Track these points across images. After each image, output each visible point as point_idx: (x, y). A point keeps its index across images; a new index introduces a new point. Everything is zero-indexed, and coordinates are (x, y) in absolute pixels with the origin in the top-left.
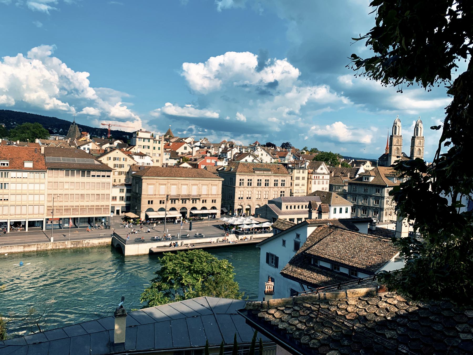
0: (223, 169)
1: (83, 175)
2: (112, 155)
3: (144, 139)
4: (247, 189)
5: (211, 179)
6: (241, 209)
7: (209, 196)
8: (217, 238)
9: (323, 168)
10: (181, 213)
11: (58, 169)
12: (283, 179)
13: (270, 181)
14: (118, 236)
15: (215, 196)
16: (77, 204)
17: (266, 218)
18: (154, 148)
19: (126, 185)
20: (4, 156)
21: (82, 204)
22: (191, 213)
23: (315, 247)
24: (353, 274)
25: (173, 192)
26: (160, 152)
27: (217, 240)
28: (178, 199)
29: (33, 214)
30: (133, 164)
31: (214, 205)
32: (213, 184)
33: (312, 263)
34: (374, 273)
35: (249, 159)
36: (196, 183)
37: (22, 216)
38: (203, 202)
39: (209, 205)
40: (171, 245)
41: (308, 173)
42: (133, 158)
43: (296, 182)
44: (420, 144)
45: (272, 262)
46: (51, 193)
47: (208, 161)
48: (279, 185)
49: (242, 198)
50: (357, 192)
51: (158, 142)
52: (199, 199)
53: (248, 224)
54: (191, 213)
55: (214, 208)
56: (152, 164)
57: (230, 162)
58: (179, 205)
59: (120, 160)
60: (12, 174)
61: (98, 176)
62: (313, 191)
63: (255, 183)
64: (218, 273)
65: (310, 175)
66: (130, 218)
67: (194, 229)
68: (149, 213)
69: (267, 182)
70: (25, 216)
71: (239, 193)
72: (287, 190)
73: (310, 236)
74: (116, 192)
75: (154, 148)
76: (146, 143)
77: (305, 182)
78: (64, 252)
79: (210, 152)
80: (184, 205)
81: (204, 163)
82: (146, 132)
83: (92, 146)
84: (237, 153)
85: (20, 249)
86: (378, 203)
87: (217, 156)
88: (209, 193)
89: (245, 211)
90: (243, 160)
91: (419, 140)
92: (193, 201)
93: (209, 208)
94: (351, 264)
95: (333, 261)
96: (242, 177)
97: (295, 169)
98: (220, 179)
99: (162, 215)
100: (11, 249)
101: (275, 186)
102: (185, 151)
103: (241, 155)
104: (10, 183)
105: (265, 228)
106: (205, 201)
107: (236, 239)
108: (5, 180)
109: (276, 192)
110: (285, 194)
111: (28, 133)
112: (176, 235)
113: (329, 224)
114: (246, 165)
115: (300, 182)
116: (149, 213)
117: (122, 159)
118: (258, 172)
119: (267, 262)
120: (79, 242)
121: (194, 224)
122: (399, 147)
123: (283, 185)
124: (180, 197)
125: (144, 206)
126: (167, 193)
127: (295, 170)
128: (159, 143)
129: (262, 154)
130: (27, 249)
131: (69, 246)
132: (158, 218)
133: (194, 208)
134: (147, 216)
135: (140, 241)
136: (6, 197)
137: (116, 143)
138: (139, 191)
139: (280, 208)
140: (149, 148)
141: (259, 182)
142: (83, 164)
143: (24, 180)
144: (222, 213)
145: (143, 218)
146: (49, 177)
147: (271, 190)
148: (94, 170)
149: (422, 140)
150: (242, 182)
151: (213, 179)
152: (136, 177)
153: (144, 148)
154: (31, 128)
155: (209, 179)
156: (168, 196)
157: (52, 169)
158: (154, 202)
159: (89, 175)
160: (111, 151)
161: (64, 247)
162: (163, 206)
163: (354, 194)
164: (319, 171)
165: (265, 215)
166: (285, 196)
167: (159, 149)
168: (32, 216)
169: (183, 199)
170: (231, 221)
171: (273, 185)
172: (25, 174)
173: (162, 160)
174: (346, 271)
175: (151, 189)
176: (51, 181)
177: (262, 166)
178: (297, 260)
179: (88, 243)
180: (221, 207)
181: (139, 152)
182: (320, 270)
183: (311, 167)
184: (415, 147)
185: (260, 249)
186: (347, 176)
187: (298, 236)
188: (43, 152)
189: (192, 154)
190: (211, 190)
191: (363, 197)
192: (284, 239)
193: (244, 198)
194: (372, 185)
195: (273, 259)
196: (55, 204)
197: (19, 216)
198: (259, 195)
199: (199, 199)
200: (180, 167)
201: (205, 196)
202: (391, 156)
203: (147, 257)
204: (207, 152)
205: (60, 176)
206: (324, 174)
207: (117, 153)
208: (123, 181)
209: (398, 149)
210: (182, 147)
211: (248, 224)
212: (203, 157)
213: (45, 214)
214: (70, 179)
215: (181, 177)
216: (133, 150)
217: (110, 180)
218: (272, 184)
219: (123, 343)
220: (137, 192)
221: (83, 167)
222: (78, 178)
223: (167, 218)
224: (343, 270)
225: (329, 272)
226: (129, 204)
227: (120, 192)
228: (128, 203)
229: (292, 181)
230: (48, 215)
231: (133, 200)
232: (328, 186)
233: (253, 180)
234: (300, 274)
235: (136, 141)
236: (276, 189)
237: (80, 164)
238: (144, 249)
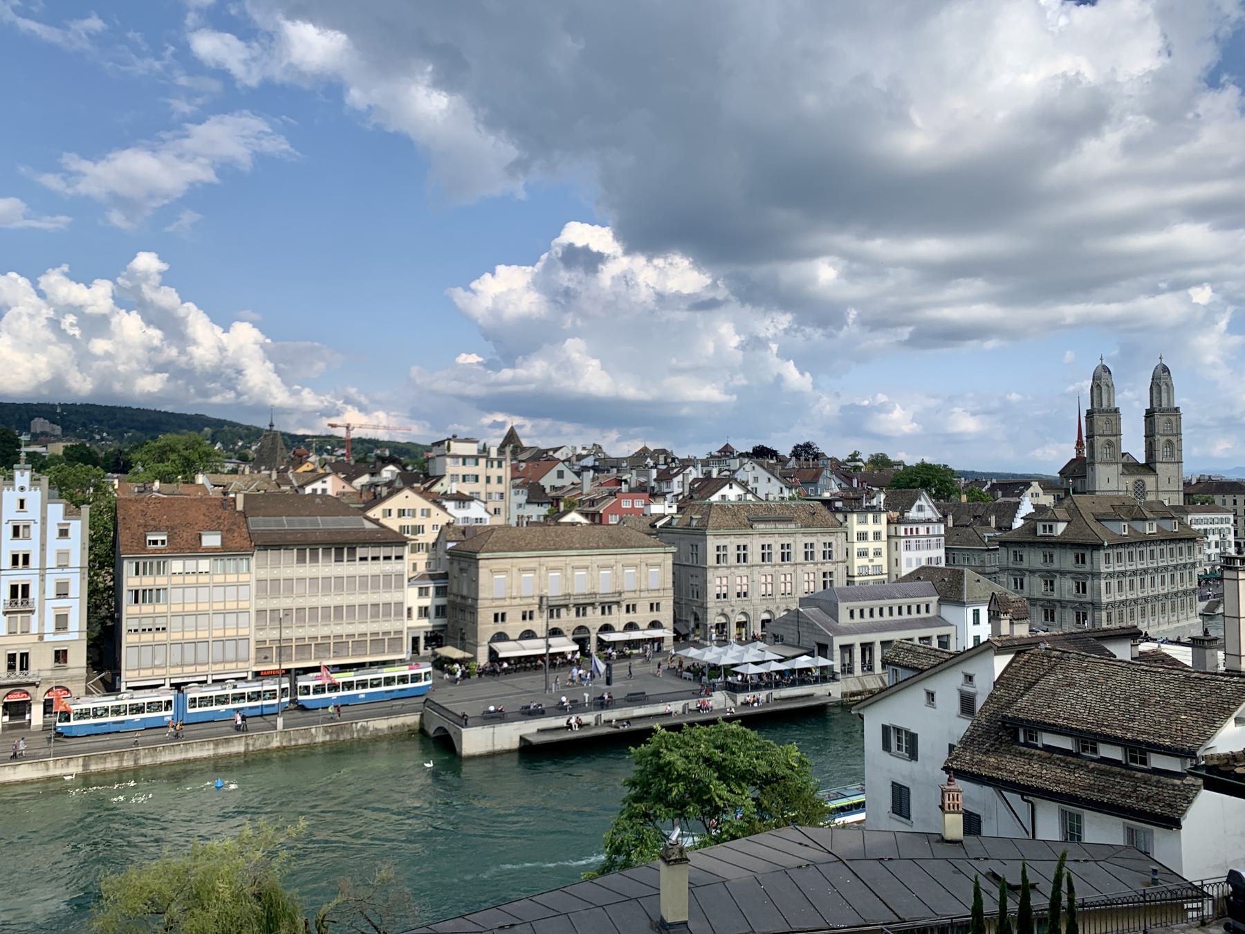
0: (669, 524)
1: (339, 559)
2: (395, 503)
3: (465, 458)
4: (737, 572)
5: (645, 550)
6: (723, 625)
7: (643, 594)
8: (683, 703)
9: (924, 508)
10: (576, 641)
11: (277, 547)
12: (828, 539)
13: (793, 546)
14: (441, 709)
15: (656, 594)
16: (325, 631)
17: (798, 647)
18: (488, 480)
19: (432, 577)
20: (152, 523)
21: (338, 630)
22: (599, 640)
23: (1024, 702)
24: (1134, 760)
25: (554, 587)
26: (501, 488)
27: (684, 707)
28: (566, 606)
29: (224, 662)
30: (448, 524)
31: (655, 616)
32: (650, 561)
33: (1022, 740)
34: (1194, 753)
35: (732, 493)
36: (607, 562)
37: (200, 668)
38: (628, 611)
39: (642, 616)
40: (569, 726)
41: (889, 522)
42: (444, 509)
43: (859, 545)
45: (899, 748)
46: (263, 607)
47: (626, 504)
48: (819, 556)
49: (725, 596)
50: (1025, 565)
51: (495, 463)
52: (618, 603)
53: (756, 663)
54: (599, 640)
55: (655, 625)
56: (489, 521)
57: (683, 505)
58: (568, 620)
59: (414, 516)
60: (177, 565)
61: (374, 558)
62: (905, 570)
63: (755, 555)
64: (783, 778)
65: (892, 527)
66: (453, 661)
67: (617, 680)
68: (497, 646)
69: (786, 551)
70: (205, 668)
71: (718, 581)
72: (840, 569)
73: (1001, 677)
74: (412, 598)
75: (488, 480)
76: (470, 469)
77: (882, 545)
78: (310, 748)
79: (626, 481)
80: (582, 621)
81: (616, 509)
82: (467, 440)
83: (332, 485)
84: (696, 480)
85: (207, 751)
86: (1084, 591)
87: (645, 491)
88: (643, 587)
89: (734, 631)
90: (715, 498)
91: (1165, 418)
92: (603, 608)
93: (643, 624)
94: (1129, 735)
95: (1081, 731)
96: (722, 542)
97: (852, 512)
98: (668, 549)
99: (534, 648)
100: (187, 750)
101: (806, 559)
102: (559, 483)
103: (708, 485)
104: (169, 587)
105: (801, 671)
106: (634, 609)
107: (730, 703)
108: (161, 581)
109: (812, 576)
110: (834, 579)
111: (174, 461)
112: (580, 701)
113: (1042, 646)
114: (724, 507)
115: (870, 545)
116: (497, 646)
117: (418, 513)
118: (762, 526)
119: (886, 746)
120: (343, 728)
121: (620, 669)
122: (1113, 439)
123: (827, 555)
124: (572, 601)
125: (486, 627)
126: (537, 592)
127: (855, 516)
128: (500, 466)
129: (756, 479)
130: (222, 750)
131: (320, 739)
132: (520, 658)
133: (607, 628)
134: (493, 654)
135: (497, 717)
136: (160, 623)
137: (389, 472)
138: (469, 588)
139: (834, 616)
140: (477, 480)
141: (767, 551)
142: (338, 532)
143: (203, 579)
144: (679, 637)
145: (483, 659)
146: (258, 567)
147: (799, 571)
148: (365, 544)
149: (1173, 418)
150: (722, 553)
151: (649, 550)
152: (460, 556)
153: (464, 480)
154: (180, 447)
155: (641, 550)
156: (541, 598)
157: (265, 547)
158: (507, 618)
159: (352, 559)
160: (390, 495)
161: (307, 741)
162: (528, 625)
163: (1016, 570)
164: (913, 514)
165: (796, 636)
166: (835, 585)
167: (500, 480)
168: (219, 667)
169: (577, 606)
170: (711, 655)
171: (801, 558)
172: (204, 564)
173: (508, 509)
174: (1116, 753)
175: (505, 583)
176: (264, 577)
177: (769, 509)
178: (979, 736)
179: (365, 729)
180: (675, 622)
181: (454, 492)
182: (1047, 754)
183: (890, 505)
184: (1157, 437)
185: (861, 717)
186: (989, 524)
187: (970, 678)
188: (240, 507)
189: (581, 489)
190: (647, 577)
191: (1041, 576)
192: (931, 689)
193: (729, 595)
194: (1062, 544)
195: (899, 740)
196: (287, 633)
197: (192, 669)
198: (769, 586)
199: (618, 603)
200: (559, 524)
201: (632, 595)
202: (1093, 464)
203: (516, 756)
204: (619, 482)
205: (286, 566)
206: (929, 521)
207: (407, 499)
208: (422, 568)
209: (1110, 444)
210: (554, 472)
211: (756, 663)
212: (612, 494)
213: (252, 661)
214: (309, 570)
215: (570, 548)
216: (437, 488)
217: (405, 567)
218: (798, 555)
219: (685, 923)
220: (465, 593)
221: (339, 538)
222: (326, 568)
223: (553, 655)
224: (1106, 751)
225: (1070, 759)
226: (445, 626)
227: (420, 595)
228: (440, 621)
229: (849, 545)
230: (257, 663)
231: (454, 615)
232: (941, 553)
233: (749, 547)
234: (998, 768)
235: (445, 464)
236: (810, 567)
237: (330, 532)
238: (507, 736)
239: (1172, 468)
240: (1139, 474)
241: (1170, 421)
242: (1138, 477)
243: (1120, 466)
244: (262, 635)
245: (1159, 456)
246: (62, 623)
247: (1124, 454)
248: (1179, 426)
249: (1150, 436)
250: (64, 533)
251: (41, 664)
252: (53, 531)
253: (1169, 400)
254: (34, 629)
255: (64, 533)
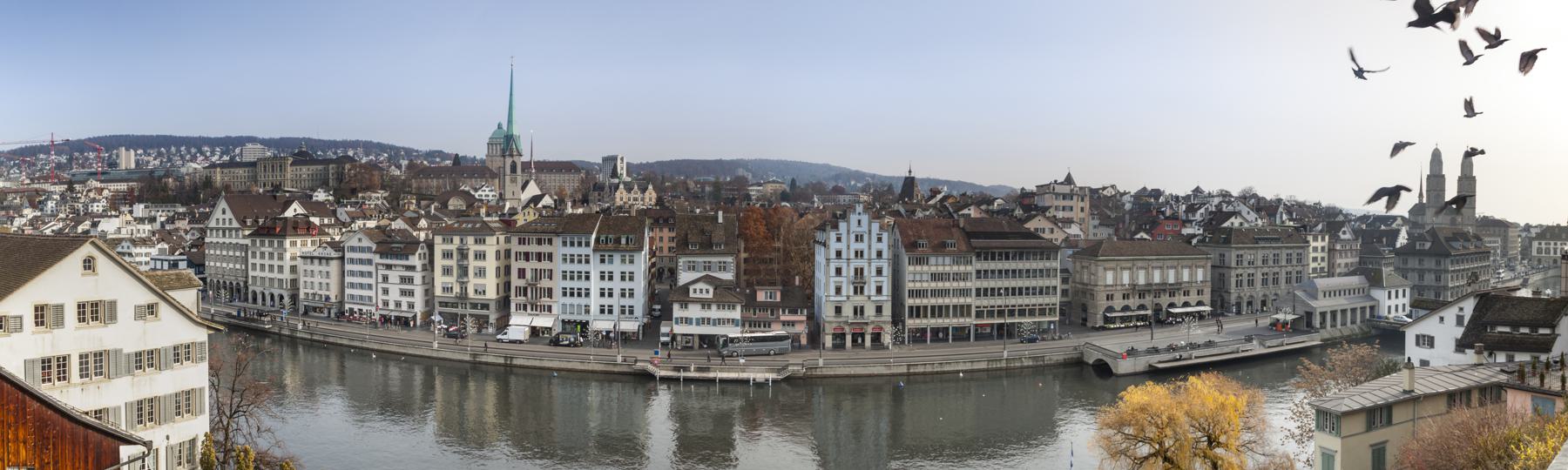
26: (1082, 215)
76: (1067, 203)
244: (978, 303)
246: (879, 290)
250: (880, 240)
251: (870, 311)
252: (874, 238)
254: (866, 292)
255: (880, 240)
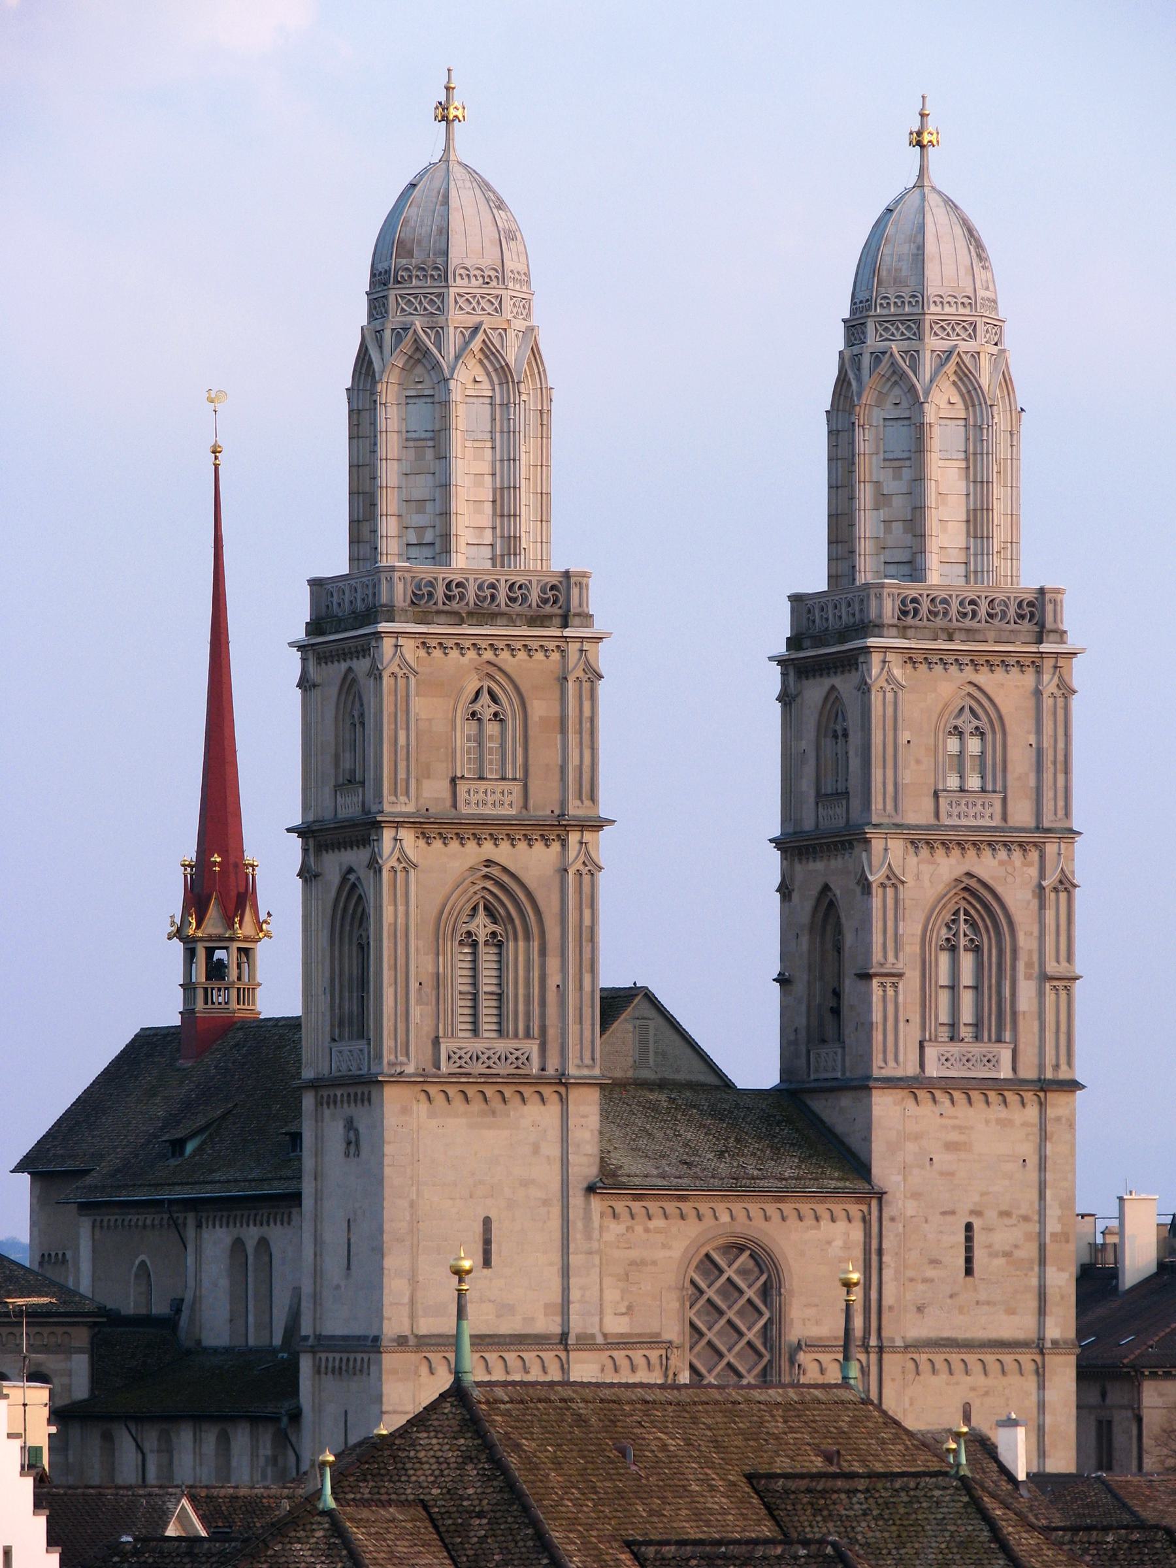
44: (993, 769)
91: (947, 687)
122: (533, 862)
149: (1009, 690)
184: (887, 854)
202: (360, 1087)
209: (504, 908)
239: (996, 1135)
240: (739, 1187)
241: (979, 717)
242: (729, 1217)
243: (587, 1109)
245: (902, 1023)
247: (614, 1003)
248: (1054, 763)
249: (823, 837)
253: (977, 521)
